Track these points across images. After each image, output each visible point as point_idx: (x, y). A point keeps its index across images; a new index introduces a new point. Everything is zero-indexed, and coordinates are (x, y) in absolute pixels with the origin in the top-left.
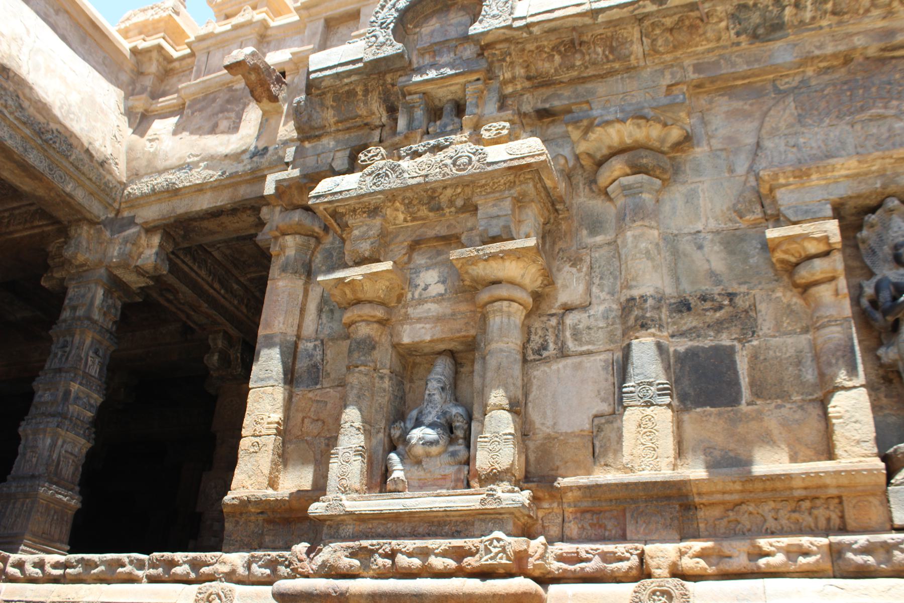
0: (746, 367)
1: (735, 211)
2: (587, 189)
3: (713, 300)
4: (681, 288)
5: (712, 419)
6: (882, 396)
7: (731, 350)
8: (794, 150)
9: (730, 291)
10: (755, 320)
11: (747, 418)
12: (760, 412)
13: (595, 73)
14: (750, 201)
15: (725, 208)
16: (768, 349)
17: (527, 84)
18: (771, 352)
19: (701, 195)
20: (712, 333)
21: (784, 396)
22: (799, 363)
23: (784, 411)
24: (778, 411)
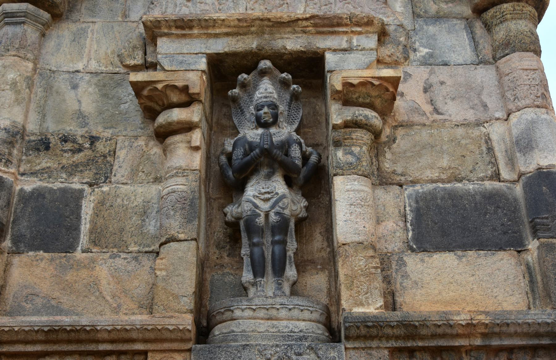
0: (90, 212)
1: (118, 56)
3: (74, 141)
4: (45, 125)
5: (42, 265)
6: (225, 255)
7: (79, 195)
9: (94, 134)
10: (112, 165)
11: (80, 265)
12: (93, 261)
14: (134, 48)
15: (109, 51)
16: (117, 196)
18: (119, 200)
19: (90, 35)
20: (64, 176)
21: (121, 246)
22: (144, 214)
23: (119, 262)
24: (111, 260)
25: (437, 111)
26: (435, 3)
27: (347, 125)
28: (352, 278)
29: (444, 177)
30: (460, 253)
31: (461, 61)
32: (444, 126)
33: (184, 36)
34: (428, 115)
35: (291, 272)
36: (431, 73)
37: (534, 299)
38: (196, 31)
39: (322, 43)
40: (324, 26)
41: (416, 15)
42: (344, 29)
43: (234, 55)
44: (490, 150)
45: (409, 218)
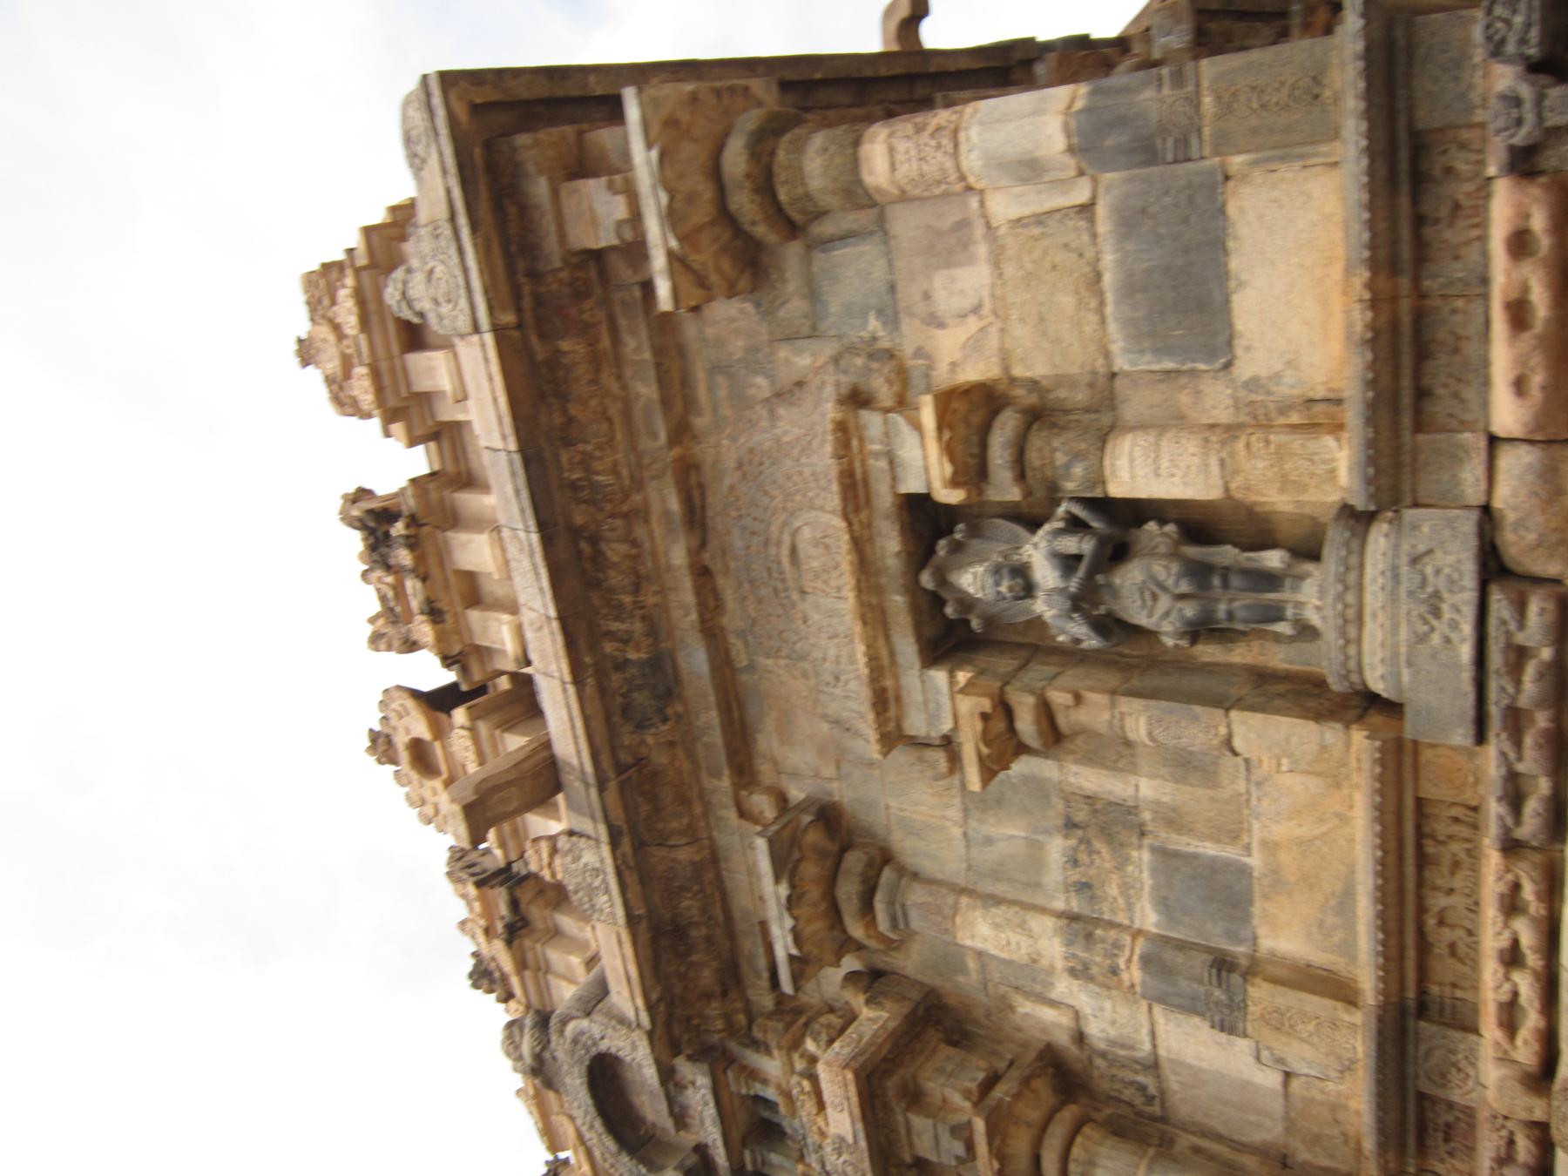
2: (895, 954)
3: (1075, 850)
8: (843, 678)
13: (718, 905)
17: (734, 994)
19: (907, 814)
20: (1130, 869)
25: (976, 310)
26: (787, 301)
27: (1021, 476)
28: (1285, 483)
29: (1093, 304)
30: (1232, 284)
31: (882, 262)
32: (1003, 298)
33: (898, 699)
34: (984, 323)
35: (1273, 559)
36: (912, 315)
37: (1315, 155)
38: (889, 683)
39: (884, 499)
40: (856, 497)
41: (814, 334)
42: (857, 464)
43: (918, 628)
44: (1040, 219)
45: (1169, 365)
